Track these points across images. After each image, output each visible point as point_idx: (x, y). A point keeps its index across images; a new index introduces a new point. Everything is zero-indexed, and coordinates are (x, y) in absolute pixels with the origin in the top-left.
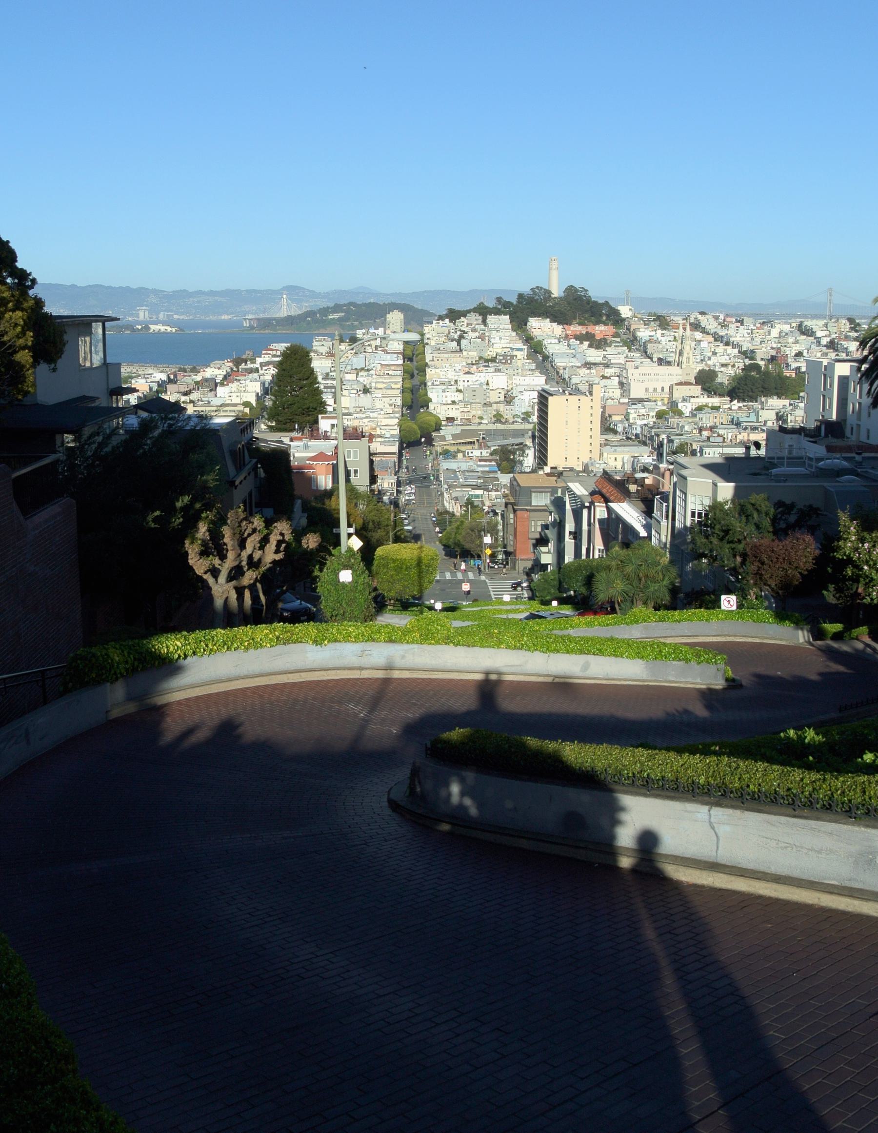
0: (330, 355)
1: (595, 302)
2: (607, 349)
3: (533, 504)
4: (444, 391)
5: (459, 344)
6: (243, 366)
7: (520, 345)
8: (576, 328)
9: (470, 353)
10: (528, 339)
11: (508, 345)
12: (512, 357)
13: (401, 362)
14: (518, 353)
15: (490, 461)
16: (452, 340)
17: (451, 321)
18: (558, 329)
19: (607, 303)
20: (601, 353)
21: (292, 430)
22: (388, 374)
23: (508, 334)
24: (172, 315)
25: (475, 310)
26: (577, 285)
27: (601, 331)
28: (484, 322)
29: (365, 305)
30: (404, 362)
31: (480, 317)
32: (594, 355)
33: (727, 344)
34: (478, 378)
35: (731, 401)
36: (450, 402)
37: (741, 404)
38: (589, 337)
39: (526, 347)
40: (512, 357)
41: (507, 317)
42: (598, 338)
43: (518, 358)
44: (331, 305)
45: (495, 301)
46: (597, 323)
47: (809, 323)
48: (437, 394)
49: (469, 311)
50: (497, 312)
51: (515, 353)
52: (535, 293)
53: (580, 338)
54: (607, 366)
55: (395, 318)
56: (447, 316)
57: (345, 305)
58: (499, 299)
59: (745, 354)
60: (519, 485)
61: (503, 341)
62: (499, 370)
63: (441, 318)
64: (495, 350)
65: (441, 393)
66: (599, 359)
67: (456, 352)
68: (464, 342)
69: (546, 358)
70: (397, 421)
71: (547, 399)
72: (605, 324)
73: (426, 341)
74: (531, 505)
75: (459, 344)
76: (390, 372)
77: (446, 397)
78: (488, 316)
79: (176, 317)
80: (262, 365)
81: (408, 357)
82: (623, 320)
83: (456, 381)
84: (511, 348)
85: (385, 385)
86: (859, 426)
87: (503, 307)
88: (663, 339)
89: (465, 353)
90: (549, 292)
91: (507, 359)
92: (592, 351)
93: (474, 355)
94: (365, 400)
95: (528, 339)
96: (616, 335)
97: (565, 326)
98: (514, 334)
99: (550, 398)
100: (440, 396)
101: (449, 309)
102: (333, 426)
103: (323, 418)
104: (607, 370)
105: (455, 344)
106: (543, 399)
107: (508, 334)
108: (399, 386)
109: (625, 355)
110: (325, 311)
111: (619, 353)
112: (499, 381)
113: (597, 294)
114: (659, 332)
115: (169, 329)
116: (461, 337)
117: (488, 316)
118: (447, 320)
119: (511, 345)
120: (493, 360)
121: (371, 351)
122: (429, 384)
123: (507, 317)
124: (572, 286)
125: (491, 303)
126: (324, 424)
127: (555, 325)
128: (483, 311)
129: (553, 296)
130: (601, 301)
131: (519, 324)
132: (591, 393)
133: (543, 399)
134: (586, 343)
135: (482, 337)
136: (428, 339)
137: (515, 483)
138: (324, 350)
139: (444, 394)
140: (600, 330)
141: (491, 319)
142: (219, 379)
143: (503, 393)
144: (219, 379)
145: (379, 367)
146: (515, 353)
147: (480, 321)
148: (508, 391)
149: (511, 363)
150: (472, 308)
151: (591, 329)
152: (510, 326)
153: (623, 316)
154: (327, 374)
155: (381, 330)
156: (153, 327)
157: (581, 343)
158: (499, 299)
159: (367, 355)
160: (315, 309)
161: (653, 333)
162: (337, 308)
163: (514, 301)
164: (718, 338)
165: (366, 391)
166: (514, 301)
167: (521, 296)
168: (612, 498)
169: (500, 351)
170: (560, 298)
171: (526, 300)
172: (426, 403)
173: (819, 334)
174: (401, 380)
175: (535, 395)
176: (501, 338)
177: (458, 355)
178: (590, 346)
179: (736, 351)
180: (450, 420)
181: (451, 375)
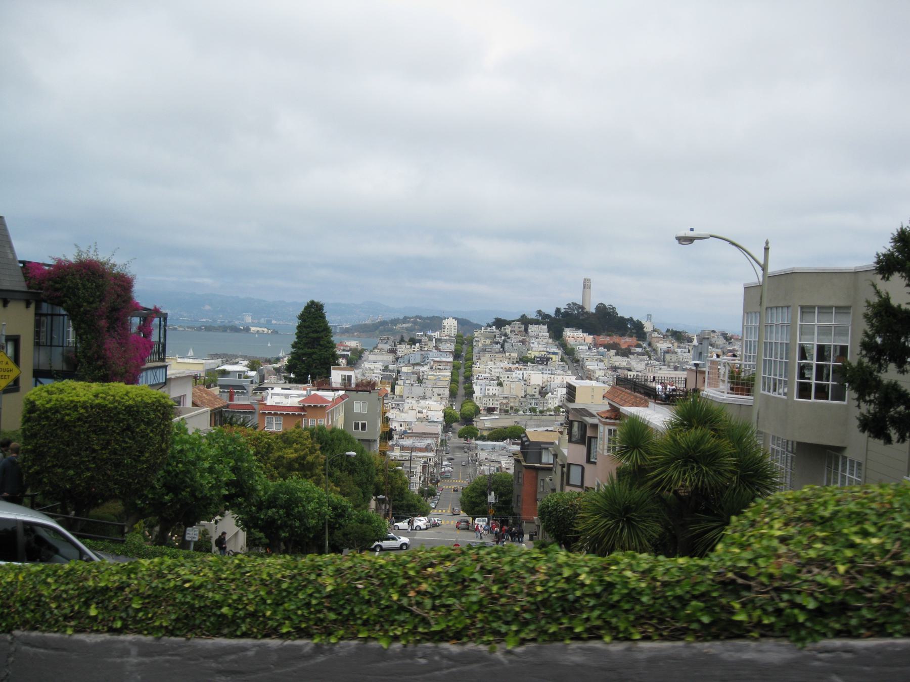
0: (393, 351)
1: (622, 318)
2: (631, 356)
3: (543, 461)
4: (487, 385)
5: (503, 346)
7: (555, 350)
9: (512, 354)
10: (563, 345)
11: (545, 349)
12: (548, 359)
13: (451, 359)
14: (553, 356)
16: (497, 343)
17: (497, 328)
18: (589, 338)
19: (631, 320)
20: (625, 359)
21: (306, 382)
22: (439, 369)
24: (271, 321)
25: (518, 321)
27: (625, 342)
28: (526, 330)
29: (428, 318)
30: (454, 360)
31: (523, 326)
32: (620, 361)
34: (517, 375)
36: (491, 394)
39: (560, 351)
40: (548, 359)
41: (546, 327)
43: (554, 359)
44: (401, 317)
45: (536, 314)
46: (623, 335)
48: (480, 387)
49: (513, 321)
50: (536, 322)
51: (551, 356)
53: (608, 347)
54: (630, 370)
55: (450, 324)
56: (494, 324)
57: (412, 318)
58: (539, 312)
60: (528, 440)
61: (540, 346)
63: (489, 326)
64: (533, 353)
66: (624, 364)
67: (500, 352)
68: (507, 345)
69: (577, 361)
70: (442, 407)
72: (631, 336)
73: (475, 344)
74: (540, 462)
75: (503, 346)
76: (441, 367)
77: (488, 390)
78: (530, 326)
79: (273, 322)
81: (457, 355)
82: (645, 334)
83: (498, 378)
84: (547, 352)
85: (435, 378)
87: (543, 319)
88: (679, 350)
89: (507, 354)
92: (619, 358)
93: (515, 355)
94: (418, 390)
95: (563, 345)
96: (639, 346)
97: (595, 336)
98: (551, 341)
100: (483, 389)
101: (496, 319)
103: (334, 369)
104: (630, 373)
105: (499, 346)
107: (545, 341)
108: (448, 378)
109: (646, 362)
110: (395, 322)
111: (641, 360)
112: (537, 377)
114: (676, 344)
115: (266, 330)
116: (505, 341)
117: (530, 326)
118: (494, 327)
119: (548, 349)
120: (533, 361)
121: (426, 349)
122: (475, 377)
123: (546, 327)
124: (602, 304)
125: (533, 315)
126: (336, 376)
128: (525, 321)
129: (585, 311)
130: (627, 316)
131: (556, 334)
134: (613, 352)
135: (523, 342)
136: (476, 341)
138: (387, 347)
139: (487, 388)
140: (625, 341)
141: (532, 328)
143: (538, 388)
145: (432, 363)
146: (551, 356)
147: (522, 329)
148: (543, 388)
149: (547, 364)
151: (616, 339)
152: (548, 334)
154: (387, 367)
155: (437, 334)
156: (253, 329)
157: (609, 350)
159: (423, 353)
162: (406, 320)
163: (552, 313)
165: (420, 381)
166: (552, 313)
167: (558, 310)
169: (537, 354)
170: (593, 314)
171: (563, 314)
172: (470, 393)
174: (449, 374)
176: (538, 343)
177: (500, 355)
178: (617, 354)
180: (490, 410)
181: (496, 372)
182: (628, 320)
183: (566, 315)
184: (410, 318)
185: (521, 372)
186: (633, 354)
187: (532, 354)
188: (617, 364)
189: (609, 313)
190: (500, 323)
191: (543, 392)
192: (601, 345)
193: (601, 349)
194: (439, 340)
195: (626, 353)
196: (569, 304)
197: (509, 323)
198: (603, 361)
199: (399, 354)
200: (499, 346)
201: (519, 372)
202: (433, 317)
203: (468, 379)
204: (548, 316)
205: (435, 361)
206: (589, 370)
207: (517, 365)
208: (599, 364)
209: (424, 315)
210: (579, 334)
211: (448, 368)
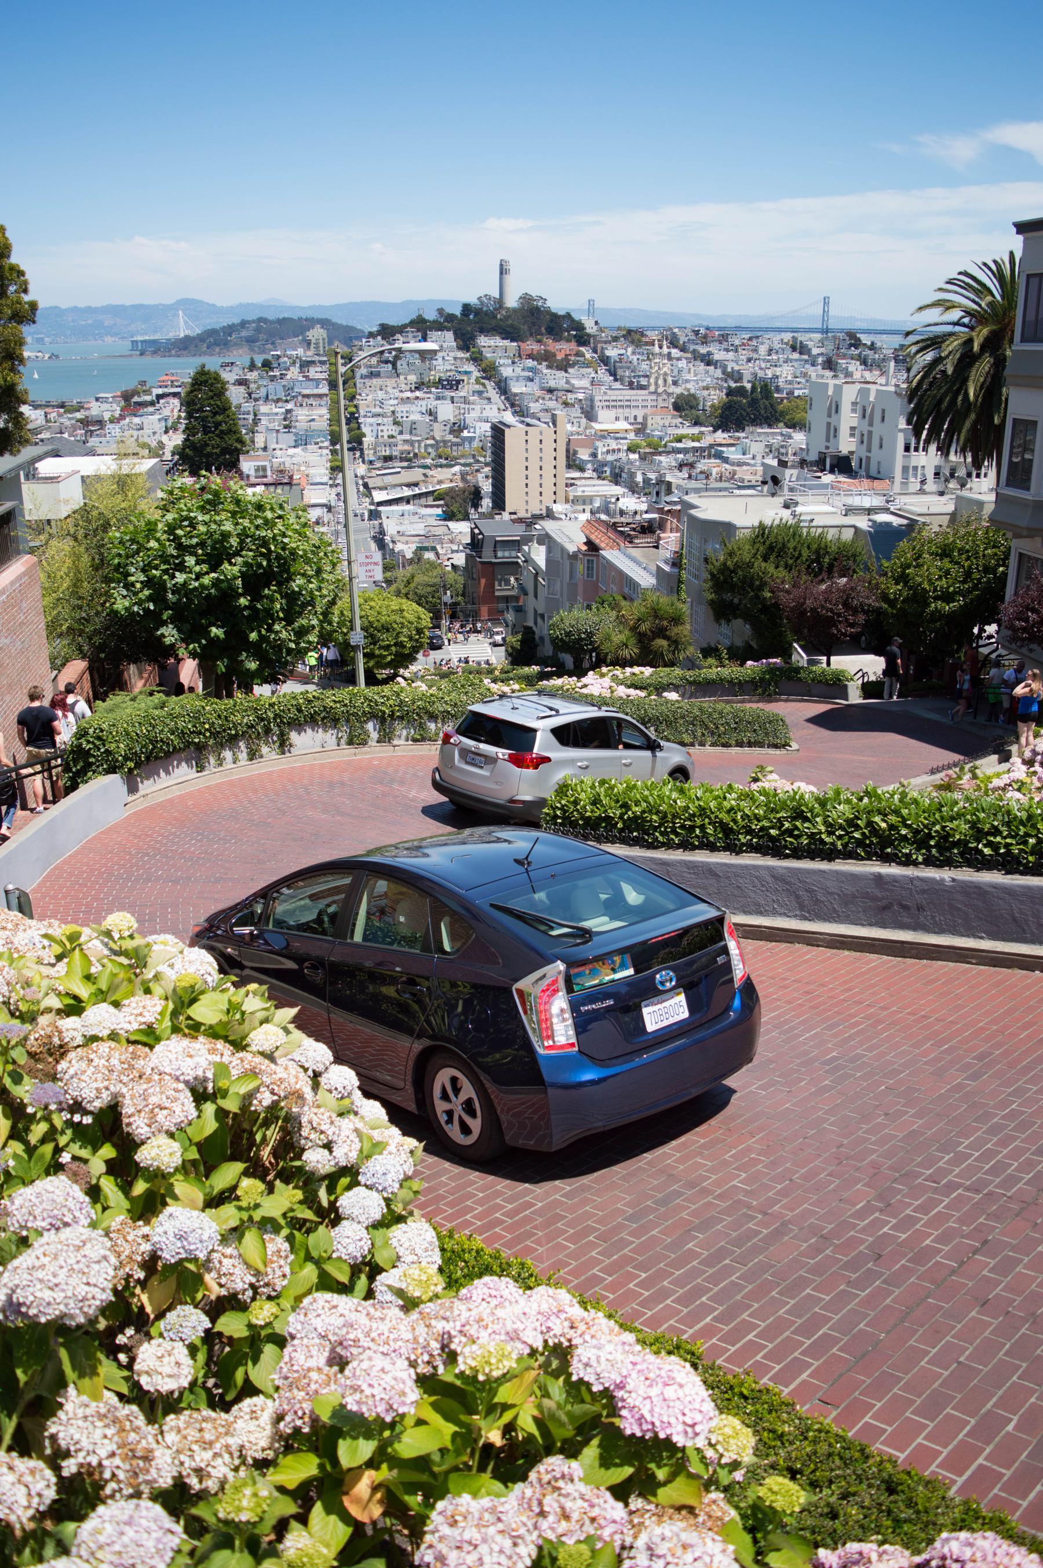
2: (570, 370)
6: (136, 399)
8: (531, 346)
10: (477, 359)
12: (458, 382)
15: (438, 506)
16: (387, 362)
19: (568, 316)
23: (452, 354)
26: (534, 294)
32: (556, 378)
33: (708, 364)
35: (714, 431)
37: (726, 435)
38: (547, 358)
40: (458, 382)
42: (559, 358)
44: (236, 320)
47: (802, 337)
49: (405, 326)
50: (439, 326)
52: (482, 303)
56: (379, 333)
57: (253, 322)
58: (440, 311)
59: (729, 375)
60: (481, 533)
62: (443, 398)
65: (375, 427)
68: (399, 363)
71: (502, 432)
72: (568, 341)
80: (159, 397)
81: (333, 385)
86: (868, 458)
87: (445, 322)
90: (500, 302)
91: (454, 384)
93: (413, 378)
99: (507, 430)
102: (257, 470)
104: (570, 396)
105: (390, 366)
106: (498, 432)
110: (230, 329)
112: (447, 411)
113: (557, 304)
116: (397, 358)
120: (439, 383)
125: (431, 315)
126: (247, 465)
127: (506, 343)
128: (422, 327)
130: (562, 313)
131: (465, 342)
132: (555, 424)
133: (498, 432)
137: (476, 531)
140: (563, 348)
142: (107, 416)
144: (107, 416)
150: (407, 321)
153: (588, 331)
158: (440, 311)
160: (217, 327)
161: (623, 352)
162: (243, 324)
163: (457, 311)
164: (697, 356)
166: (457, 311)
167: (467, 308)
168: (603, 545)
173: (815, 351)
175: (487, 427)
178: (549, 367)
179: (719, 373)
181: (390, 405)
182: (564, 317)
183: (478, 312)
184: (249, 322)
185: (424, 403)
186: (572, 366)
187: (434, 376)
188: (552, 384)
189: (537, 308)
190: (387, 332)
191: (457, 428)
192: (530, 356)
193: (530, 363)
194: (305, 365)
195: (564, 366)
196: (479, 298)
197: (401, 330)
198: (532, 380)
199: (253, 386)
200: (390, 366)
201: (421, 402)
202: (284, 319)
203: (353, 419)
204: (450, 318)
205: (304, 396)
206: (516, 395)
207: (418, 394)
208: (529, 384)
209: (271, 318)
210: (497, 341)
211: (323, 403)
